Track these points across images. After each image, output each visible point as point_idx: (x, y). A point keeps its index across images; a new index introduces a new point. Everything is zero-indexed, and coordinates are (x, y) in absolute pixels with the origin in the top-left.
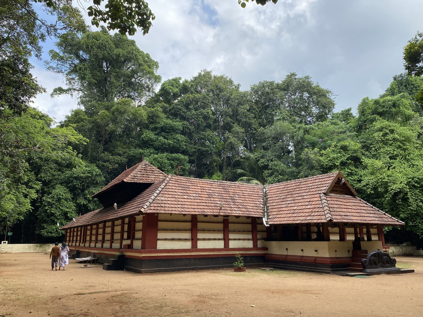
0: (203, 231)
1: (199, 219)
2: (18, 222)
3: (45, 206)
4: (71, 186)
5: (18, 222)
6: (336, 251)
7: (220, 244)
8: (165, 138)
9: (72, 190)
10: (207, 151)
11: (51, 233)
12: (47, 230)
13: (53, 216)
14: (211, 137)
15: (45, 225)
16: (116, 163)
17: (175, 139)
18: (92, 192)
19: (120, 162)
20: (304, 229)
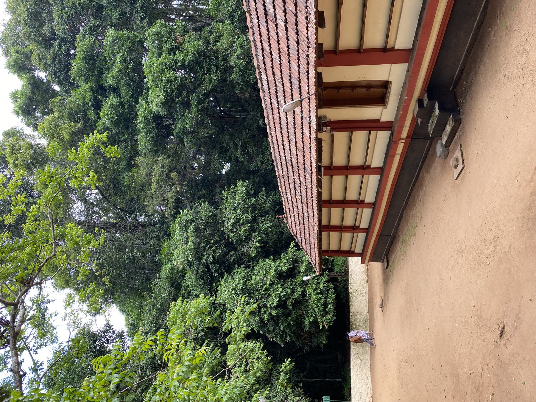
2: (300, 385)
3: (262, 321)
4: (217, 270)
5: (300, 385)
9: (226, 267)
11: (325, 305)
12: (318, 313)
13: (285, 302)
15: (307, 321)
16: (169, 178)
18: (233, 225)
19: (167, 170)
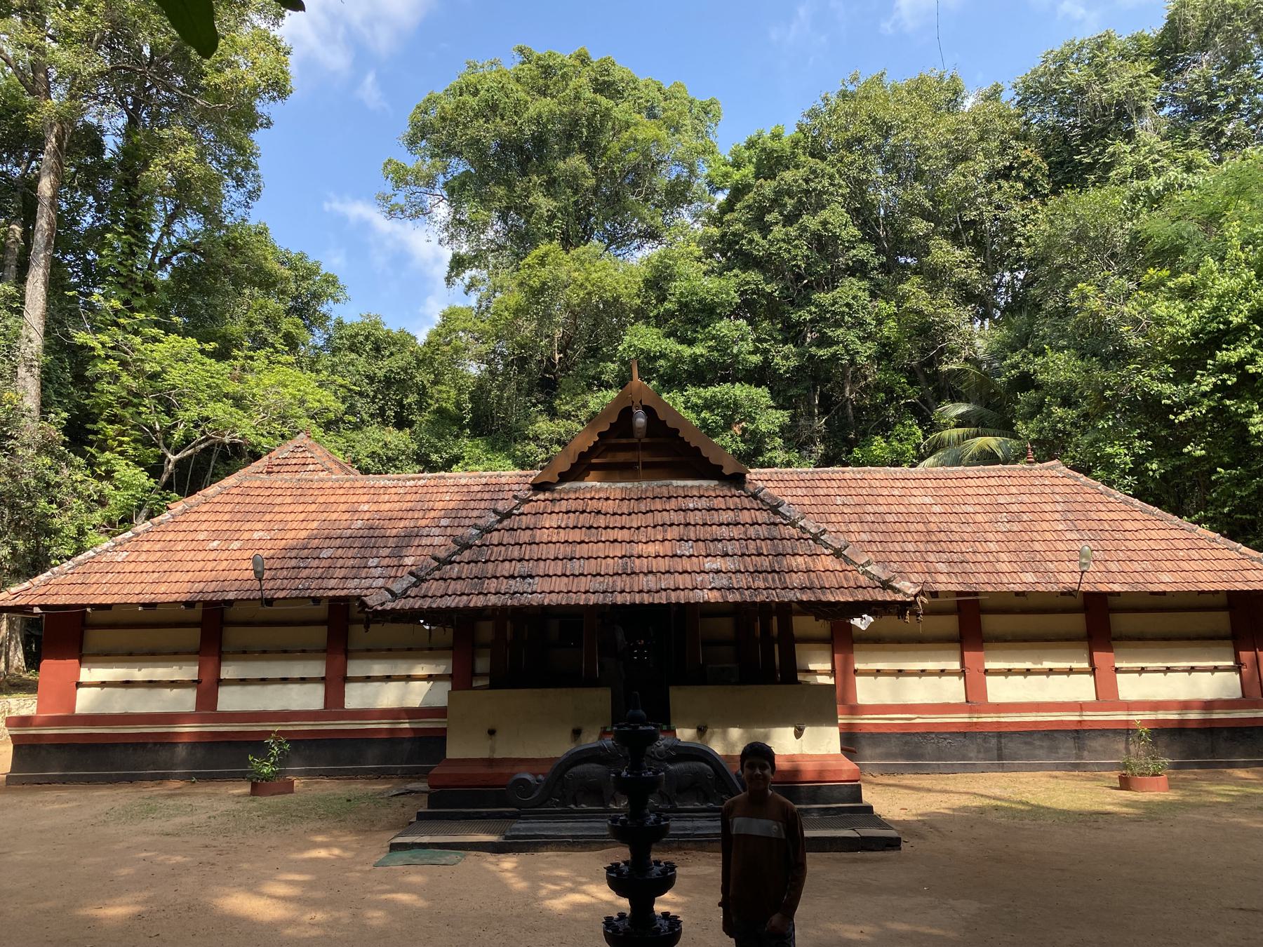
0: (244, 653)
1: (231, 613)
6: (492, 732)
7: (311, 698)
8: (683, 340)
10: (835, 358)
14: (848, 305)
17: (714, 338)
20: (725, 627)
